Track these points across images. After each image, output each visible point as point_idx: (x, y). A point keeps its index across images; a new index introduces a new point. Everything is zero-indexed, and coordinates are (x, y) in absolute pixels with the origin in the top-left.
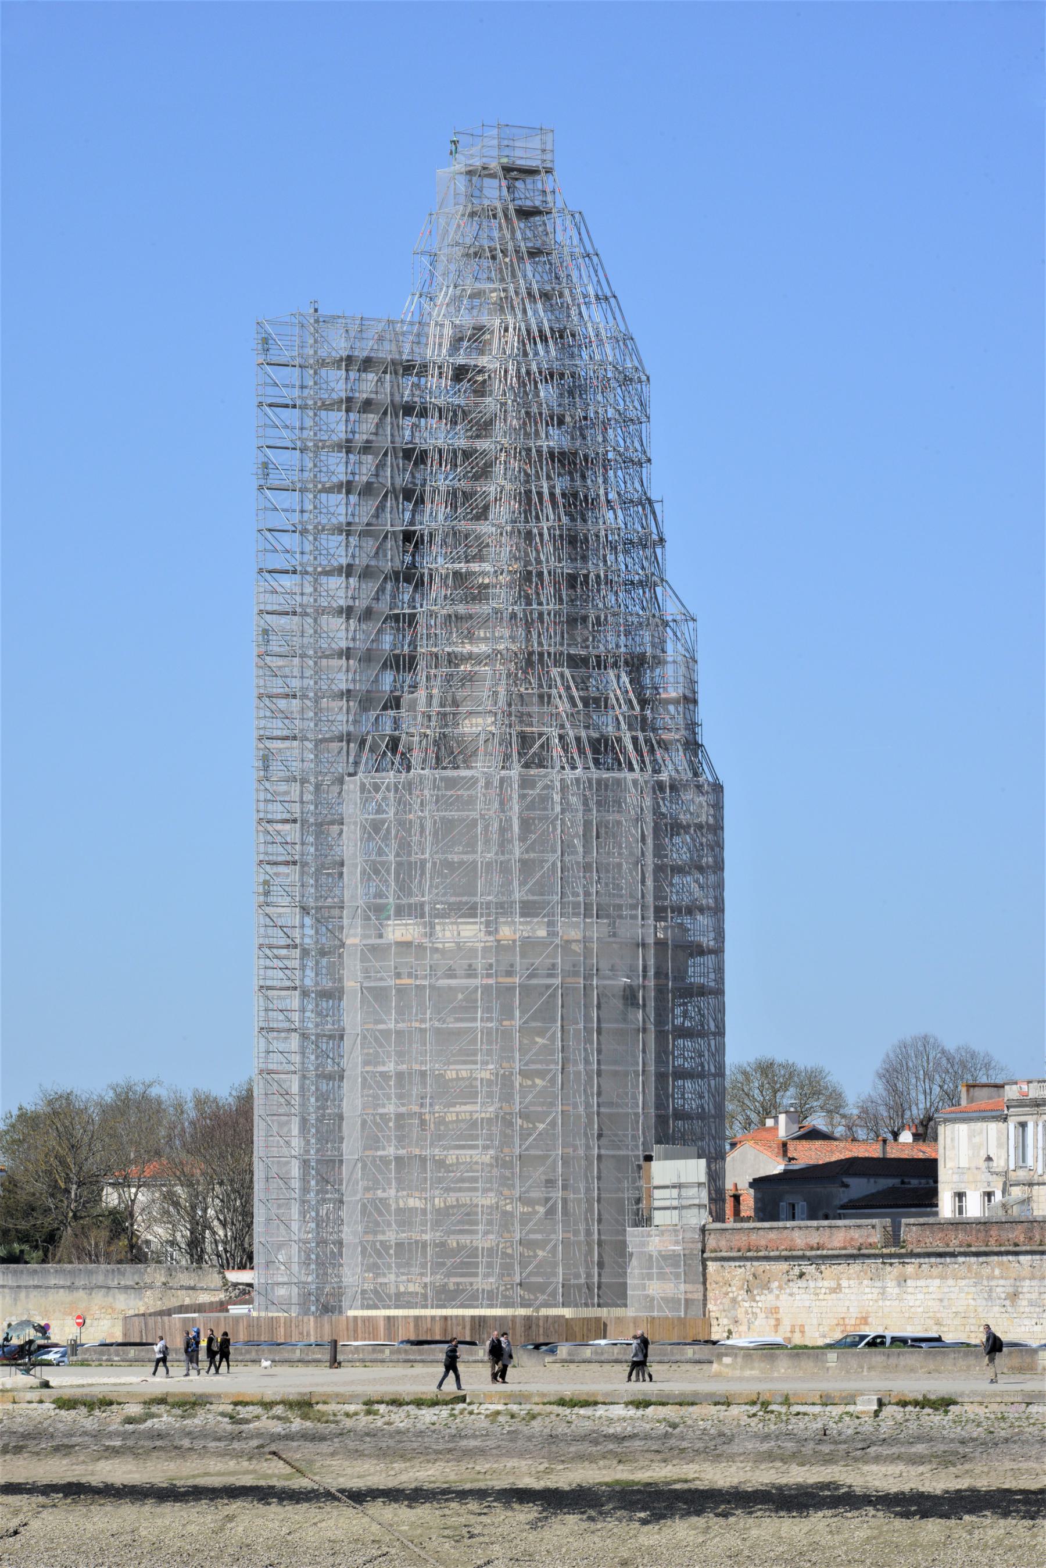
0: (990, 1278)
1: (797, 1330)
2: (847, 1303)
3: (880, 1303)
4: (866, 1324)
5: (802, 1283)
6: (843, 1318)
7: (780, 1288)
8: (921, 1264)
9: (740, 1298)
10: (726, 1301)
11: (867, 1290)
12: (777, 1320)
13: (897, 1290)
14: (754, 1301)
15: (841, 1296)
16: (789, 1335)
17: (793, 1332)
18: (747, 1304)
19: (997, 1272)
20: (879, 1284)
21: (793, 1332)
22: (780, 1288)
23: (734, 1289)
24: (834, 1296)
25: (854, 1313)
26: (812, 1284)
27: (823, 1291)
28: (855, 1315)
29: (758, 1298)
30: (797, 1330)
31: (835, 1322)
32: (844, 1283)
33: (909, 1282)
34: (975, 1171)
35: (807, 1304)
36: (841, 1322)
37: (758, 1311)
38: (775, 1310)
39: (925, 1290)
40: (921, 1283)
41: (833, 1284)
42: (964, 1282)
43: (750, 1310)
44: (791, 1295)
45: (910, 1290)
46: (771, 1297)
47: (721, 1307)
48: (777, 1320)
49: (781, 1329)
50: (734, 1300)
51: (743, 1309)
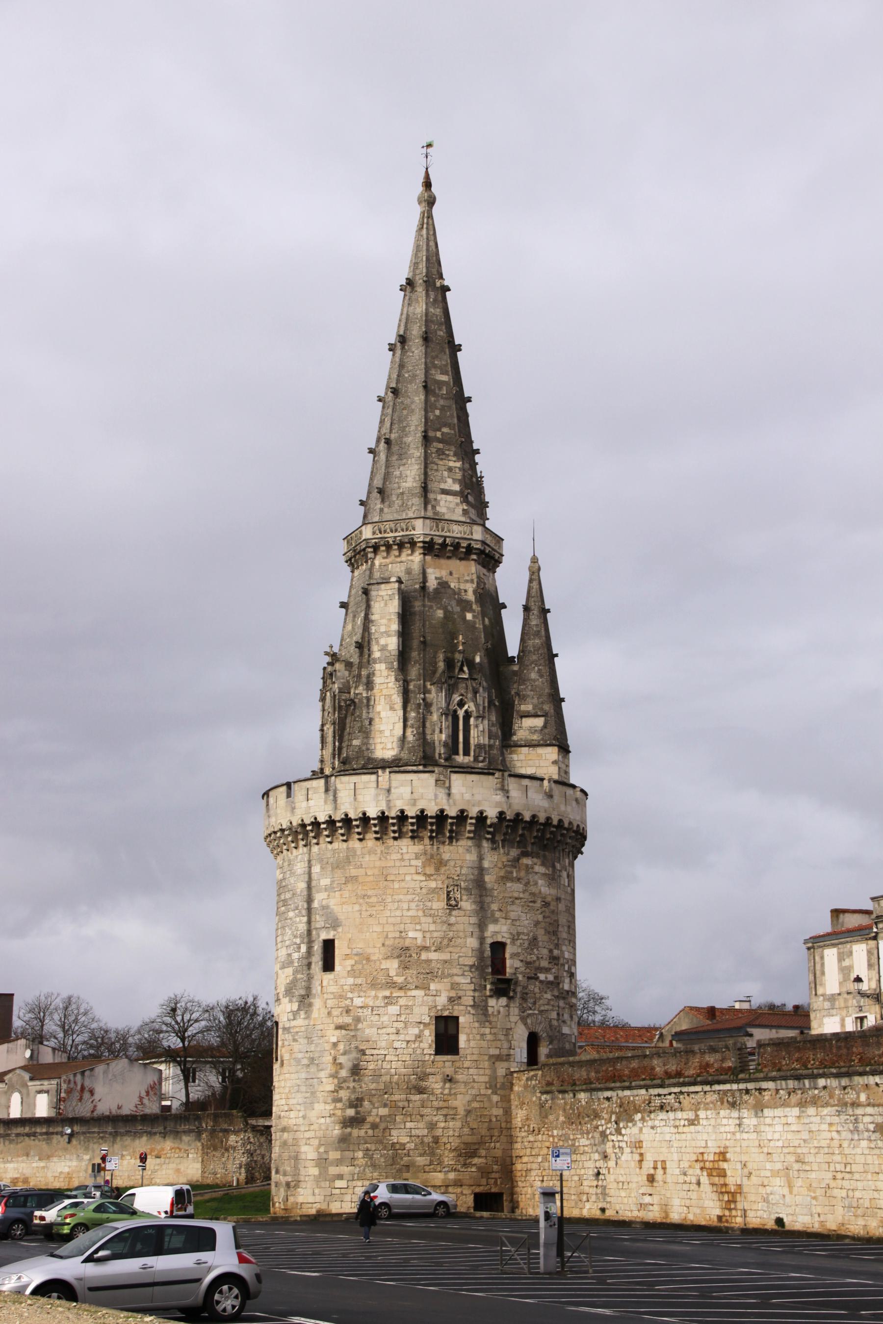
0: (855, 1104)
1: (659, 1165)
2: (705, 1137)
3: (738, 1136)
4: (725, 1160)
5: (662, 1115)
6: (702, 1154)
7: (643, 1119)
8: (777, 1091)
9: (608, 1132)
10: (597, 1135)
11: (725, 1121)
13: (754, 1121)
14: (620, 1134)
15: (699, 1128)
16: (652, 1171)
17: (655, 1168)
18: (614, 1138)
19: (863, 1097)
20: (735, 1114)
21: (655, 1168)
22: (643, 1119)
23: (603, 1122)
24: (692, 1127)
25: (713, 1148)
26: (671, 1115)
28: (713, 1150)
29: (623, 1131)
30: (659, 1165)
31: (695, 1158)
32: (702, 1114)
33: (765, 1111)
34: (845, 996)
35: (668, 1137)
36: (700, 1158)
37: (623, 1145)
38: (638, 1145)
39: (784, 1120)
40: (778, 1112)
41: (691, 1115)
42: (826, 1111)
43: (617, 1144)
44: (652, 1128)
45: (768, 1121)
46: (635, 1130)
47: (592, 1141)
48: (641, 1155)
49: (645, 1164)
50: (603, 1135)
51: (611, 1144)
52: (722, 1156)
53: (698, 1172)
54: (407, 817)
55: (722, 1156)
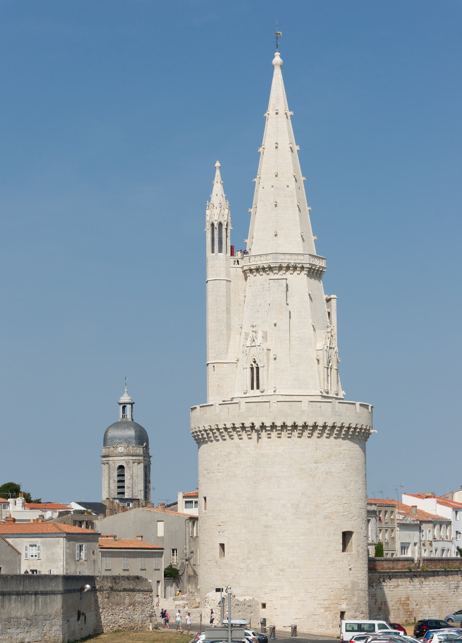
1: (383, 603)
6: (400, 598)
11: (409, 586)
12: (376, 600)
13: (419, 586)
15: (399, 589)
16: (380, 606)
17: (381, 604)
21: (381, 604)
22: (376, 585)
27: (392, 587)
28: (405, 597)
30: (383, 603)
31: (397, 600)
41: (396, 584)
45: (423, 586)
48: (376, 600)
49: (377, 603)
52: (408, 599)
53: (399, 605)
54: (317, 426)
55: (408, 599)
